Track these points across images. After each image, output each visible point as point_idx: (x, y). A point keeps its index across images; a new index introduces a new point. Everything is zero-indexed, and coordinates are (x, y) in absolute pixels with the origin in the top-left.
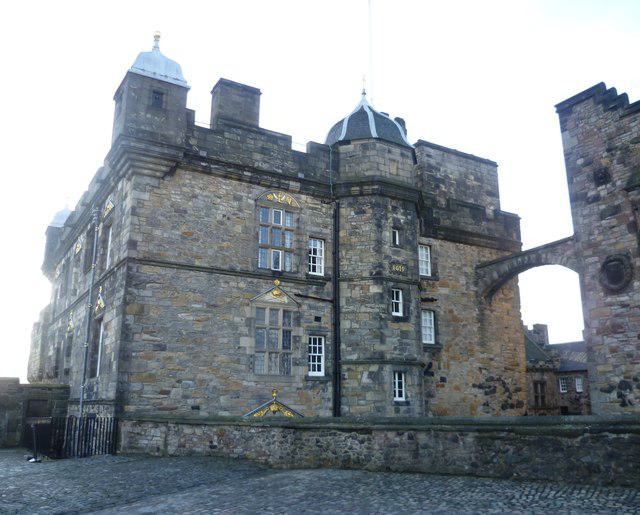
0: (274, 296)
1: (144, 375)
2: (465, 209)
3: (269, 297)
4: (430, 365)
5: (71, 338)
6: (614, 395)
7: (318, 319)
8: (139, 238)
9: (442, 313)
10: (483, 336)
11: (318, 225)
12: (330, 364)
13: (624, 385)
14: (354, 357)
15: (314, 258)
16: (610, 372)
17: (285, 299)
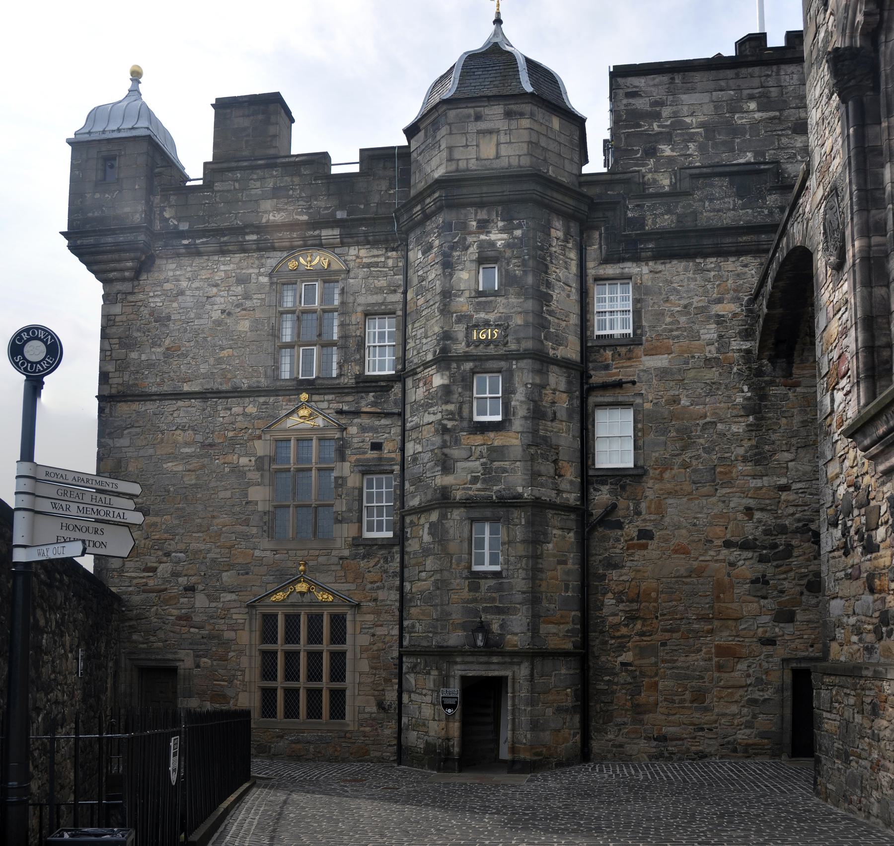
0: (302, 419)
2: (716, 181)
7: (376, 446)
8: (110, 368)
17: (320, 422)
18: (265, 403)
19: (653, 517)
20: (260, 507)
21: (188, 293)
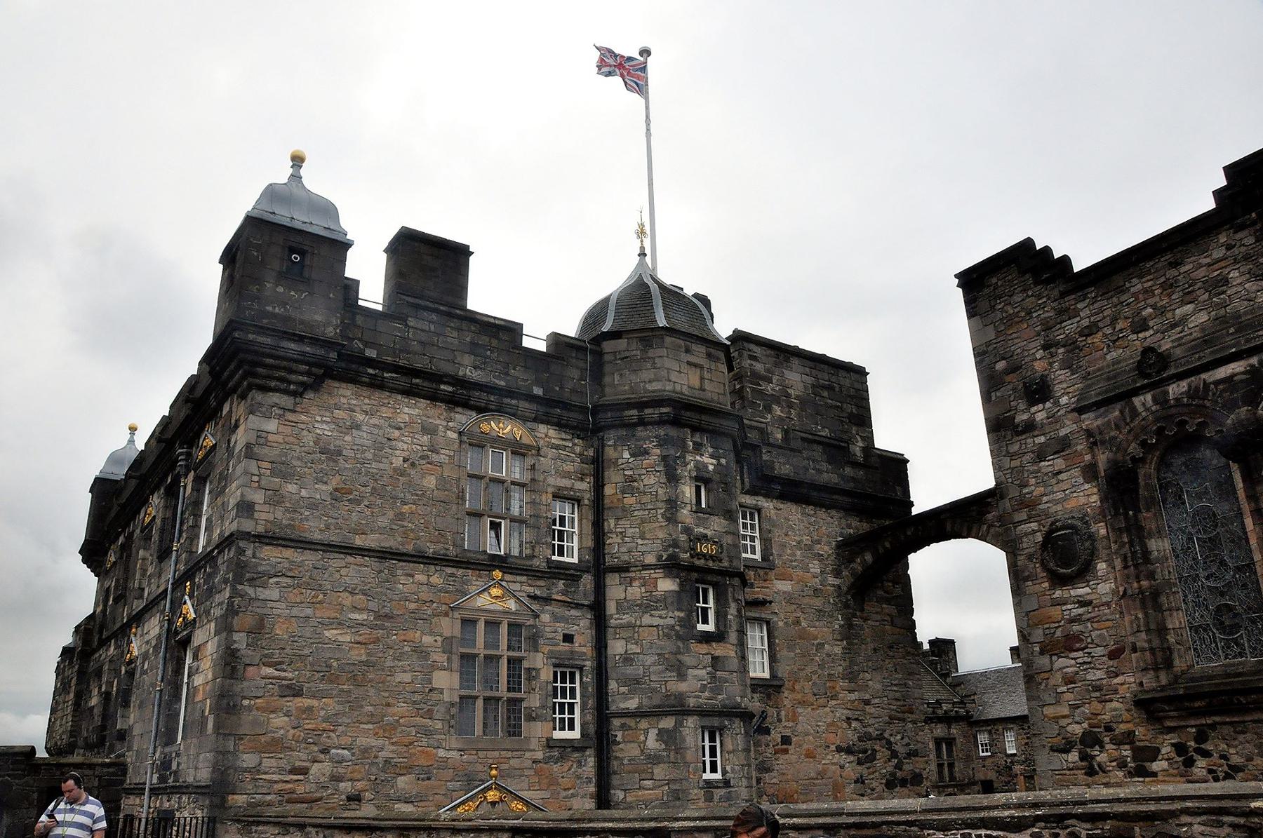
0: (491, 598)
1: (263, 739)
2: (815, 446)
3: (483, 601)
4: (763, 716)
5: (131, 674)
6: (1074, 756)
7: (568, 638)
9: (781, 624)
10: (852, 663)
11: (567, 475)
12: (589, 718)
13: (1091, 740)
14: (632, 704)
15: (561, 533)
16: (1064, 717)
17: (512, 605)
18: (452, 575)
19: (791, 724)
20: (446, 697)
21: (364, 428)
